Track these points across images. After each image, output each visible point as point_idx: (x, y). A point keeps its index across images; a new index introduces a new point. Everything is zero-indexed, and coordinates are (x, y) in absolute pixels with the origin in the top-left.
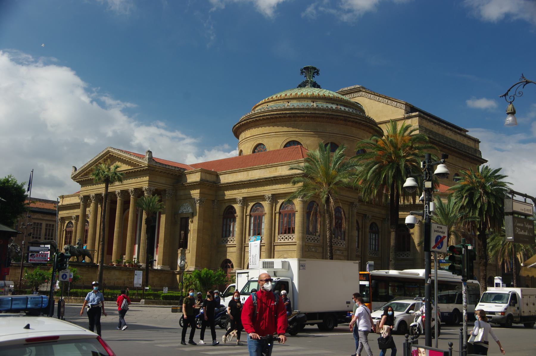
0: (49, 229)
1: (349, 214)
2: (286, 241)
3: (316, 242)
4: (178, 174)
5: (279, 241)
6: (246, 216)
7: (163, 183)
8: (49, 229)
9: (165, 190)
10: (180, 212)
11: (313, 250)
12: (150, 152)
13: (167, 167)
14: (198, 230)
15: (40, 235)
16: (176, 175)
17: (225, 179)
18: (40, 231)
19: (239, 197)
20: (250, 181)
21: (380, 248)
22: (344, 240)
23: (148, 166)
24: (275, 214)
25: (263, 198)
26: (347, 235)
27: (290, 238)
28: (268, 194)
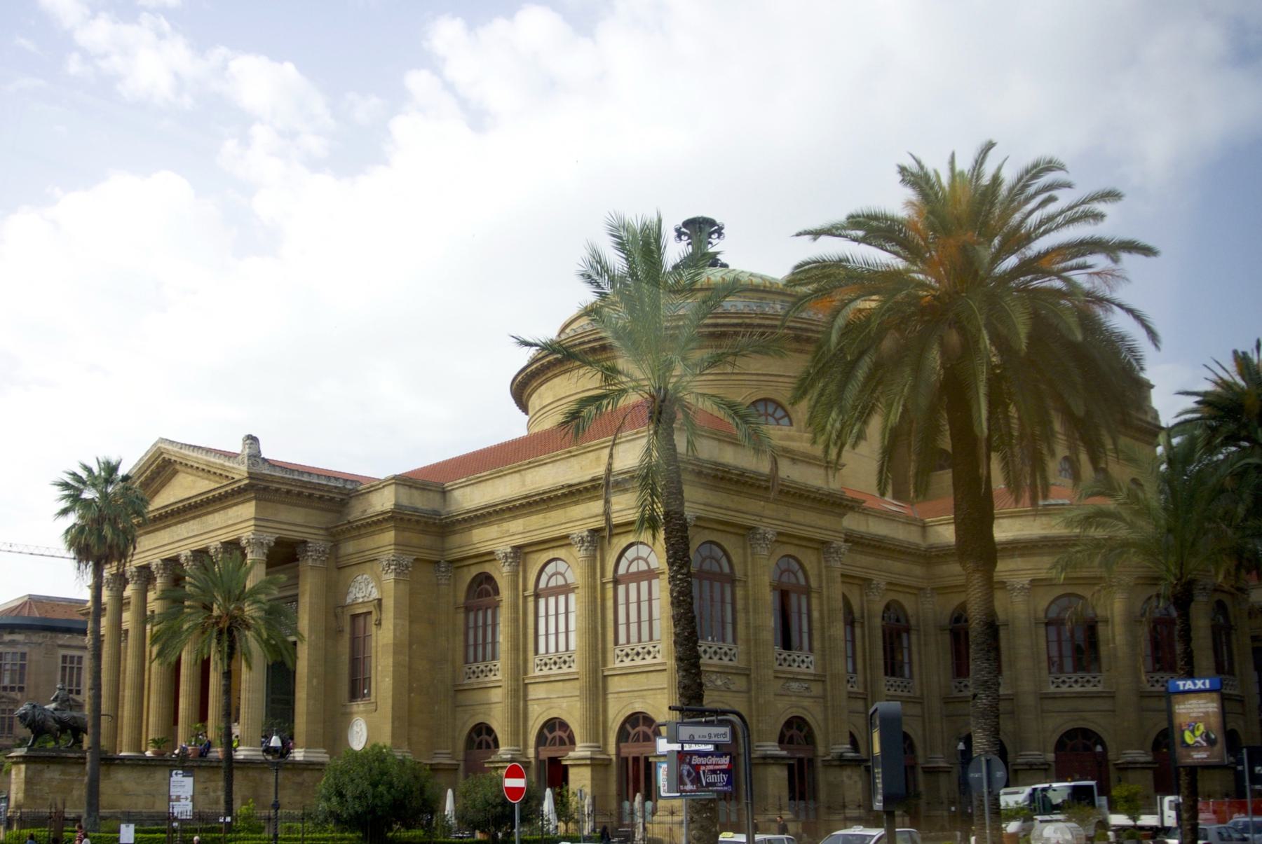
0: (72, 668)
1: (820, 575)
2: (638, 661)
3: (726, 660)
4: (338, 497)
5: (618, 664)
6: (525, 598)
7: (295, 522)
8: (72, 668)
9: (305, 542)
10: (349, 601)
11: (719, 683)
12: (252, 440)
13: (306, 478)
14: (395, 644)
15: (78, 684)
16: (332, 499)
17: (470, 497)
18: (79, 674)
19: (503, 548)
20: (526, 497)
21: (916, 669)
22: (811, 650)
23: (251, 476)
24: (603, 584)
25: (563, 541)
26: (816, 635)
27: (649, 653)
28: (579, 530)
